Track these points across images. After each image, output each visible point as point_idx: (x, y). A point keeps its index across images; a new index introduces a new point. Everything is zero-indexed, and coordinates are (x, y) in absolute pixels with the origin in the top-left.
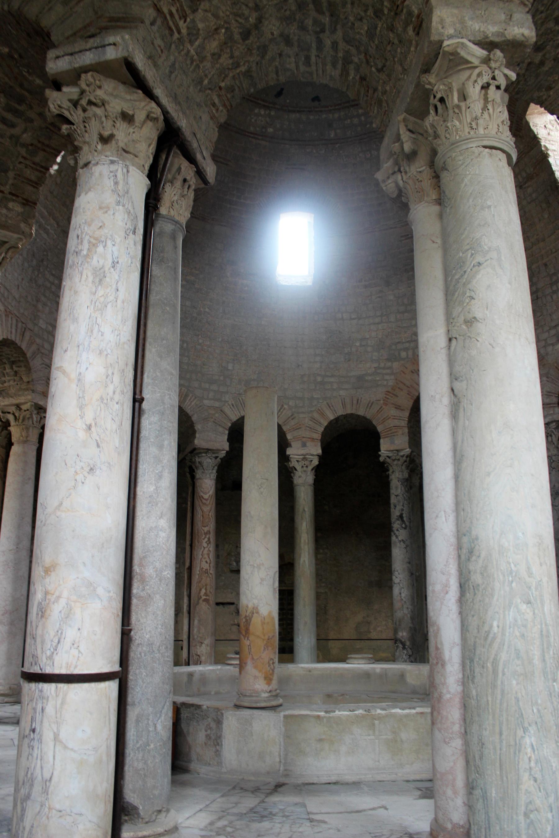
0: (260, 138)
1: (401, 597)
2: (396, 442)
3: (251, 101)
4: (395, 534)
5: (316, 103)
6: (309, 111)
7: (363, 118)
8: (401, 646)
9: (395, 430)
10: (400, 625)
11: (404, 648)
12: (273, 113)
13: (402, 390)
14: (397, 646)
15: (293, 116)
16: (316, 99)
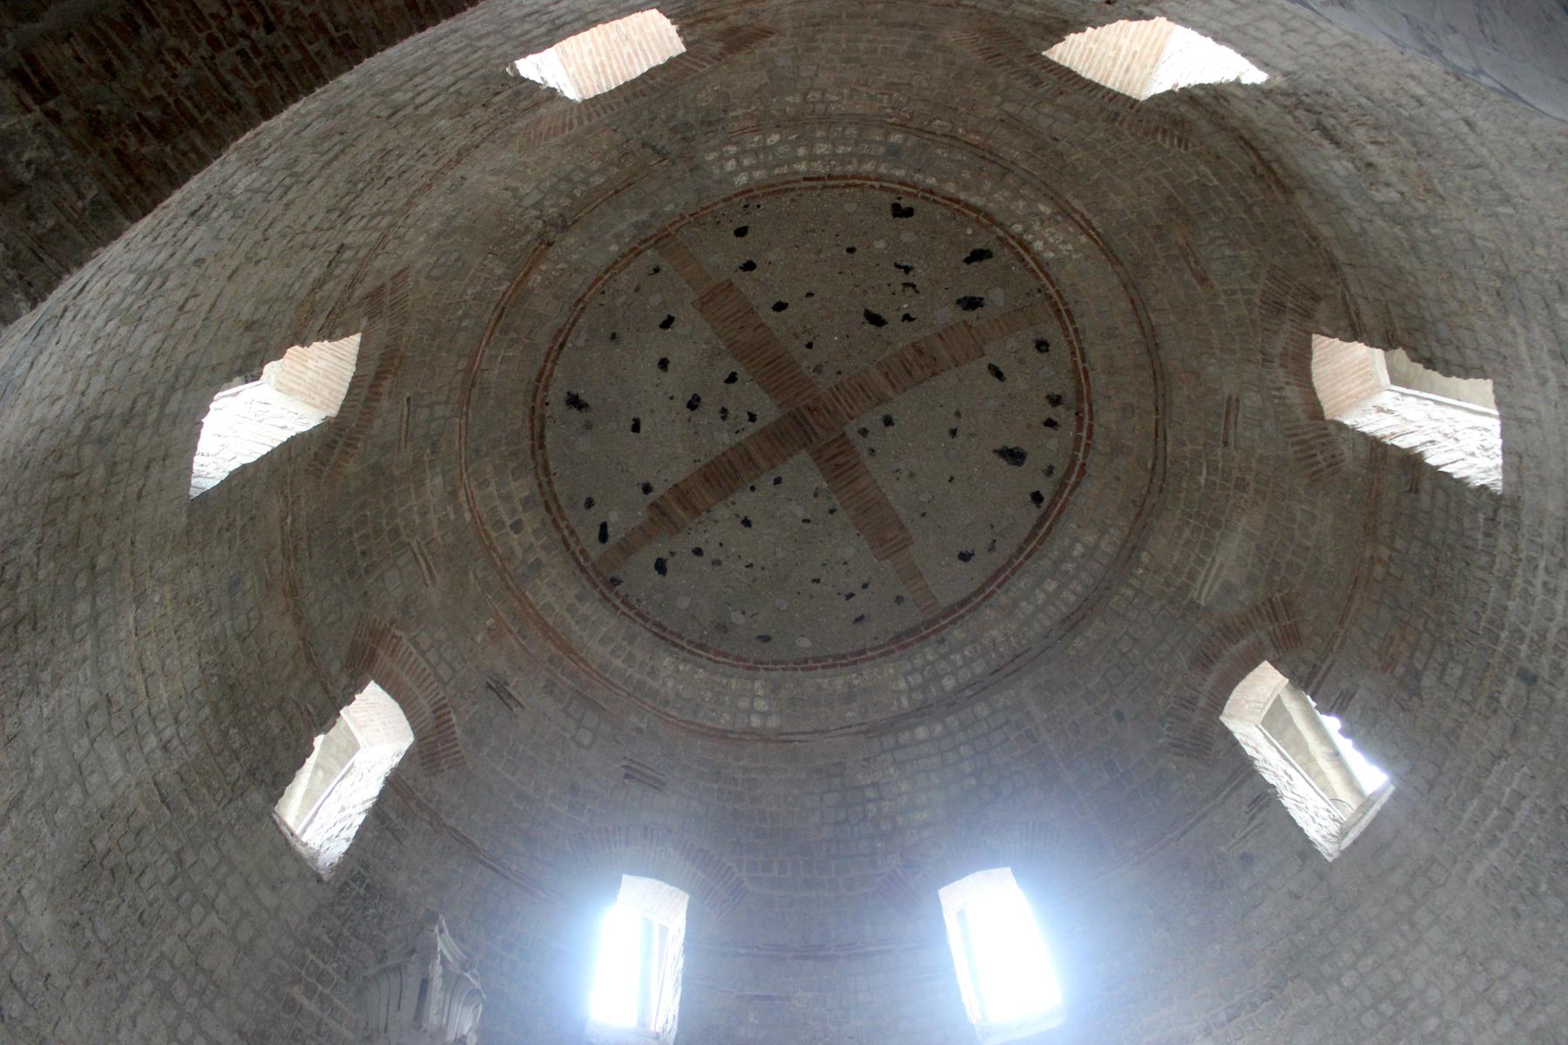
0: (1078, 218)
3: (1047, 276)
5: (904, 203)
6: (932, 192)
7: (801, 152)
12: (1018, 228)
15: (976, 200)
16: (900, 212)
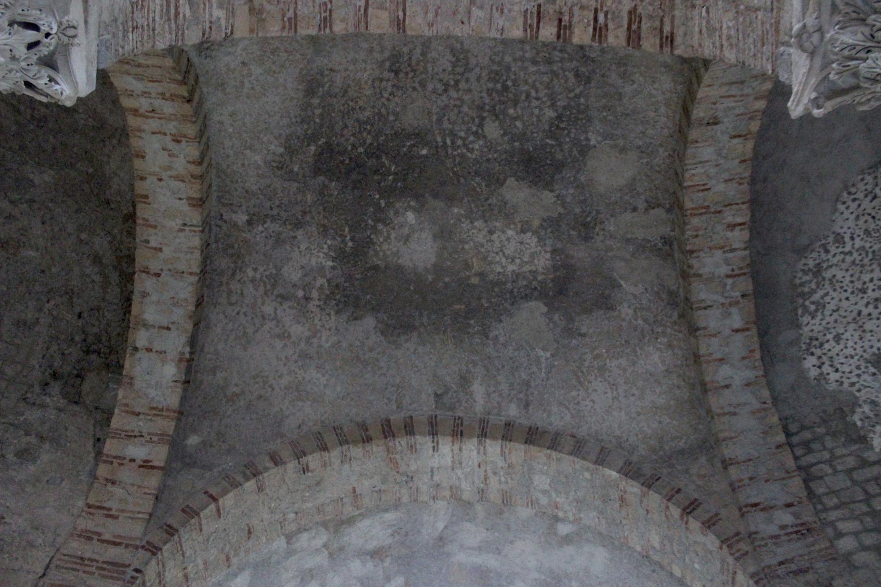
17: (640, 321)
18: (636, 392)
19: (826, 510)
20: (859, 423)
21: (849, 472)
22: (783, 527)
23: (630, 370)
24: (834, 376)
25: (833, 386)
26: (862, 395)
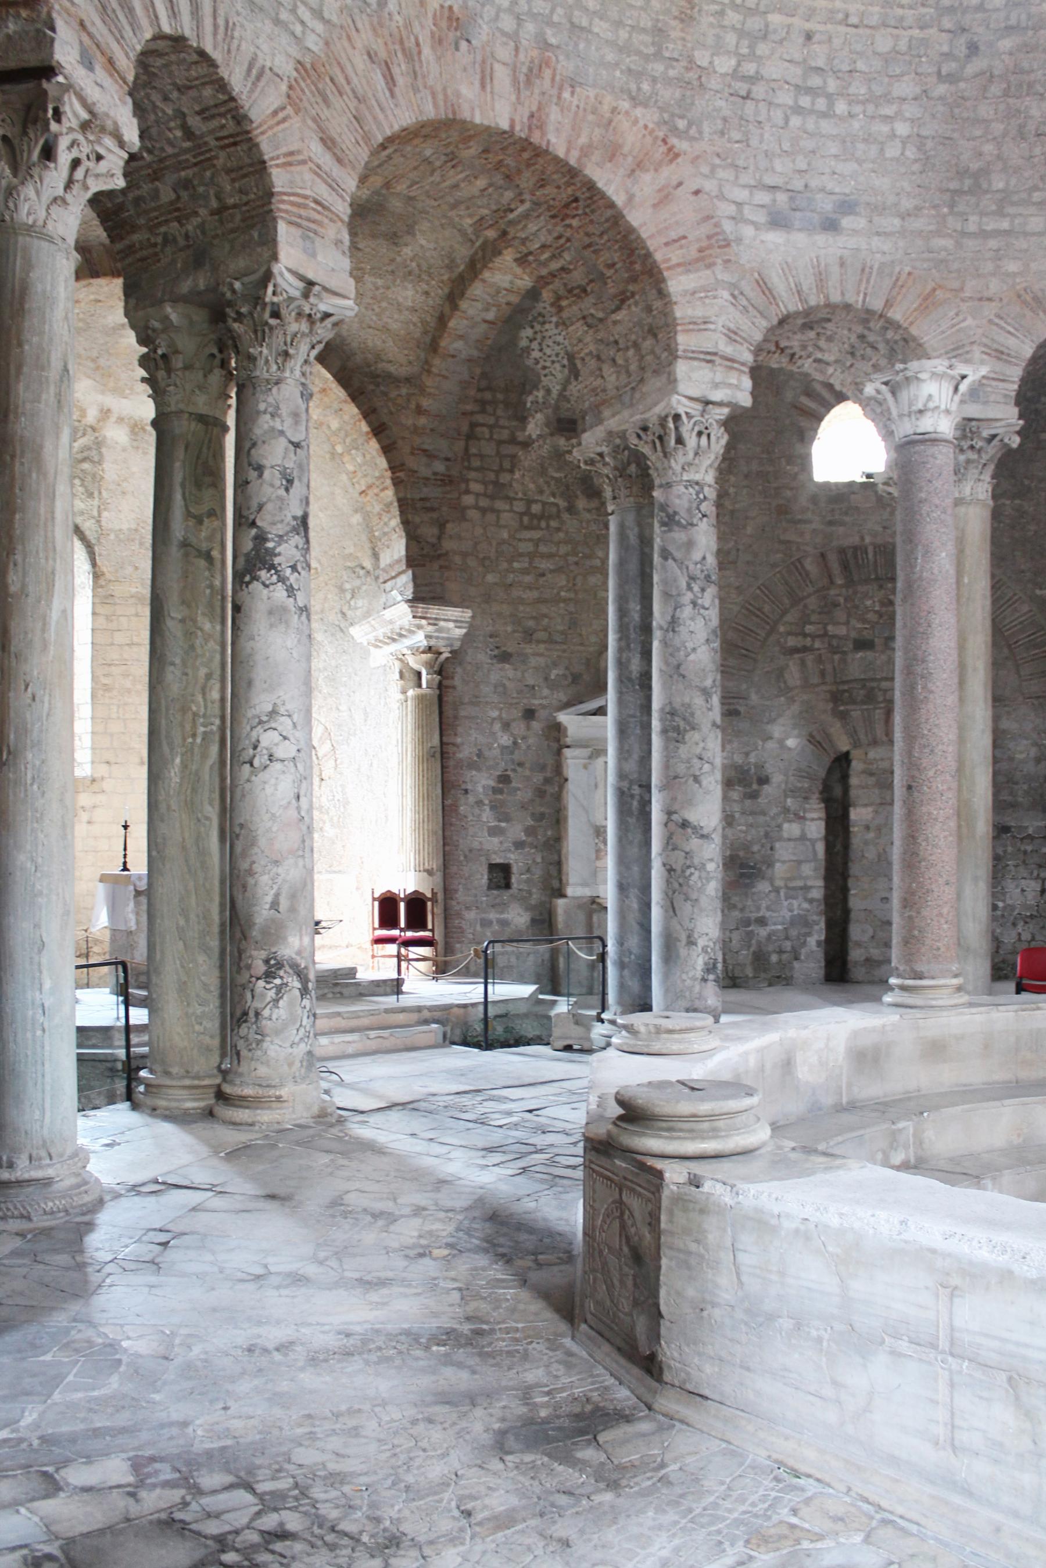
1: (298, 808)
2: (320, 258)
4: (282, 580)
8: (297, 984)
9: (318, 217)
10: (292, 910)
11: (304, 991)
13: (341, 94)
14: (279, 989)
17: (414, 264)
18: (377, 310)
19: (469, 468)
20: (529, 405)
21: (500, 443)
22: (435, 474)
23: (381, 291)
24: (536, 354)
25: (530, 362)
26: (545, 381)
